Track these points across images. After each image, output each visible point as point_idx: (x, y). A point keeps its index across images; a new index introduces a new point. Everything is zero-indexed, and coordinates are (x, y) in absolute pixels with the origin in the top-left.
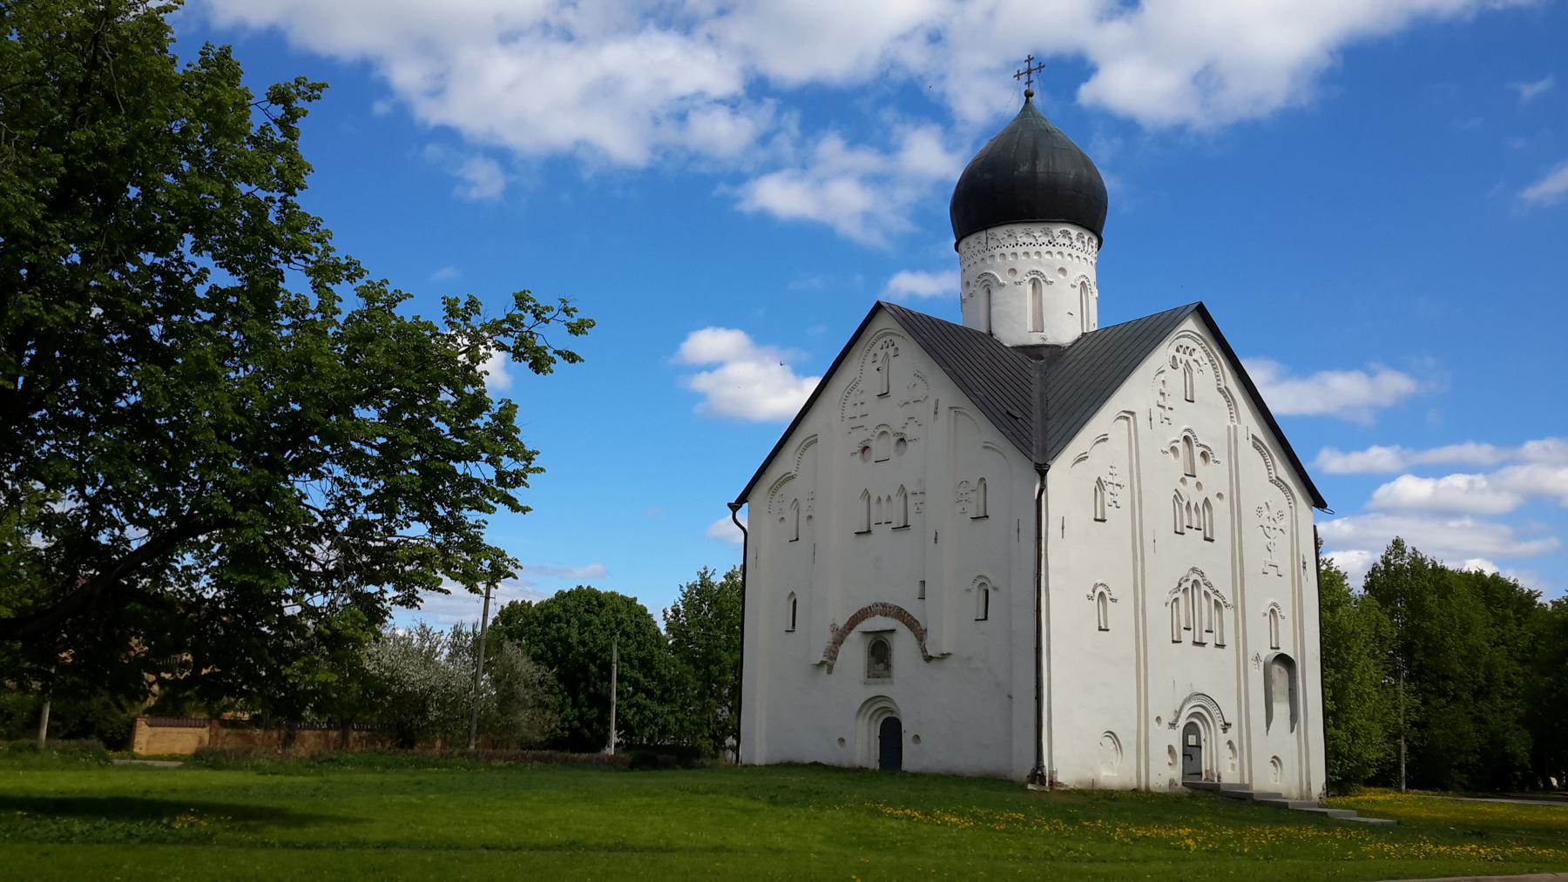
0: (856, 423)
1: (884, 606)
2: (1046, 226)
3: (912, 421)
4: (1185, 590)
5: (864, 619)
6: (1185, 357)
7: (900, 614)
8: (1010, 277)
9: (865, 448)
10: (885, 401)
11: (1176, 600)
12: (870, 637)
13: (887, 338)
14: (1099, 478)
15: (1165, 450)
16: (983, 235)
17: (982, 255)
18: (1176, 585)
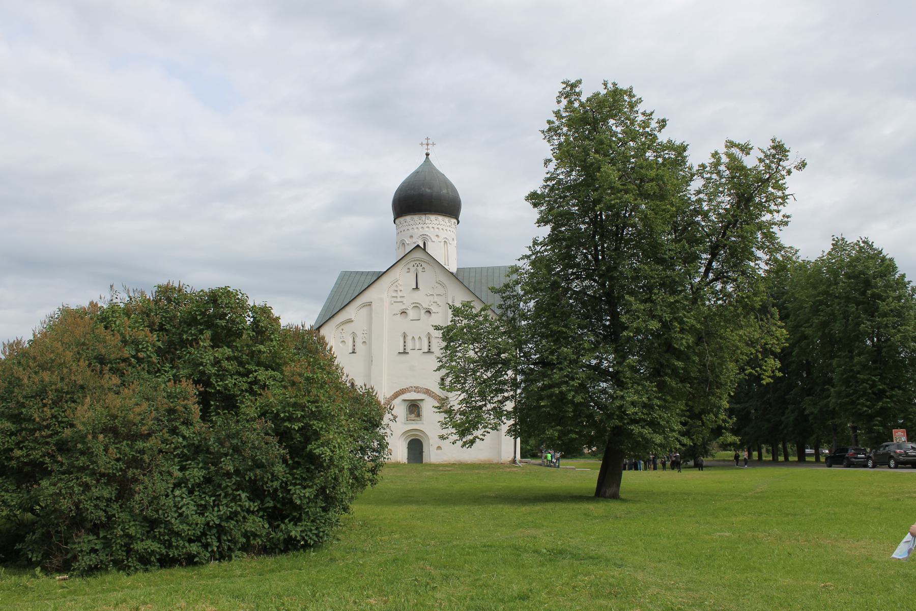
0: (399, 299)
1: (417, 388)
2: (450, 218)
3: (435, 304)
5: (403, 394)
7: (428, 392)
8: (436, 238)
9: (404, 312)
10: (417, 292)
12: (407, 403)
13: (418, 263)
16: (423, 217)
17: (422, 225)
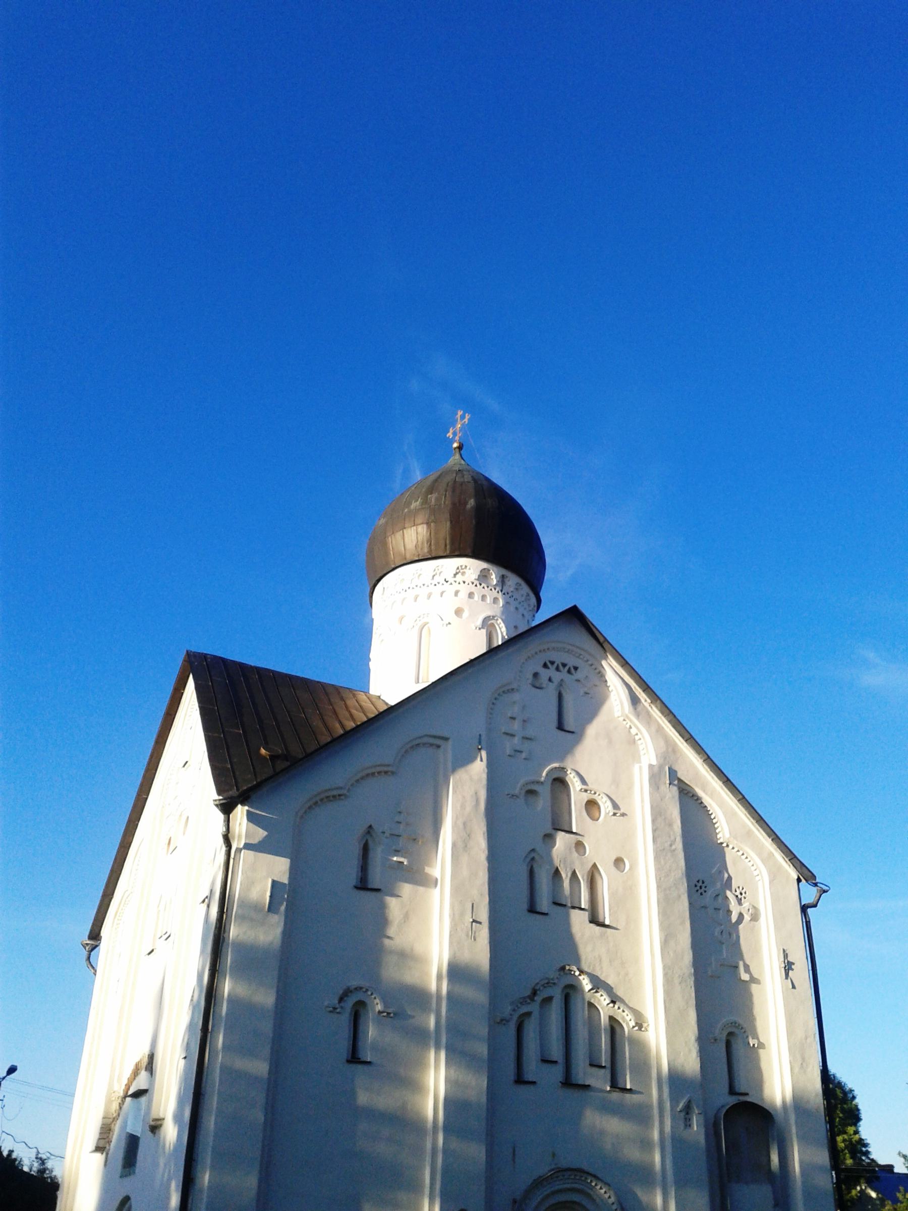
4: (549, 1000)
6: (557, 676)
11: (528, 1014)
14: (370, 827)
15: (517, 792)
18: (528, 993)
